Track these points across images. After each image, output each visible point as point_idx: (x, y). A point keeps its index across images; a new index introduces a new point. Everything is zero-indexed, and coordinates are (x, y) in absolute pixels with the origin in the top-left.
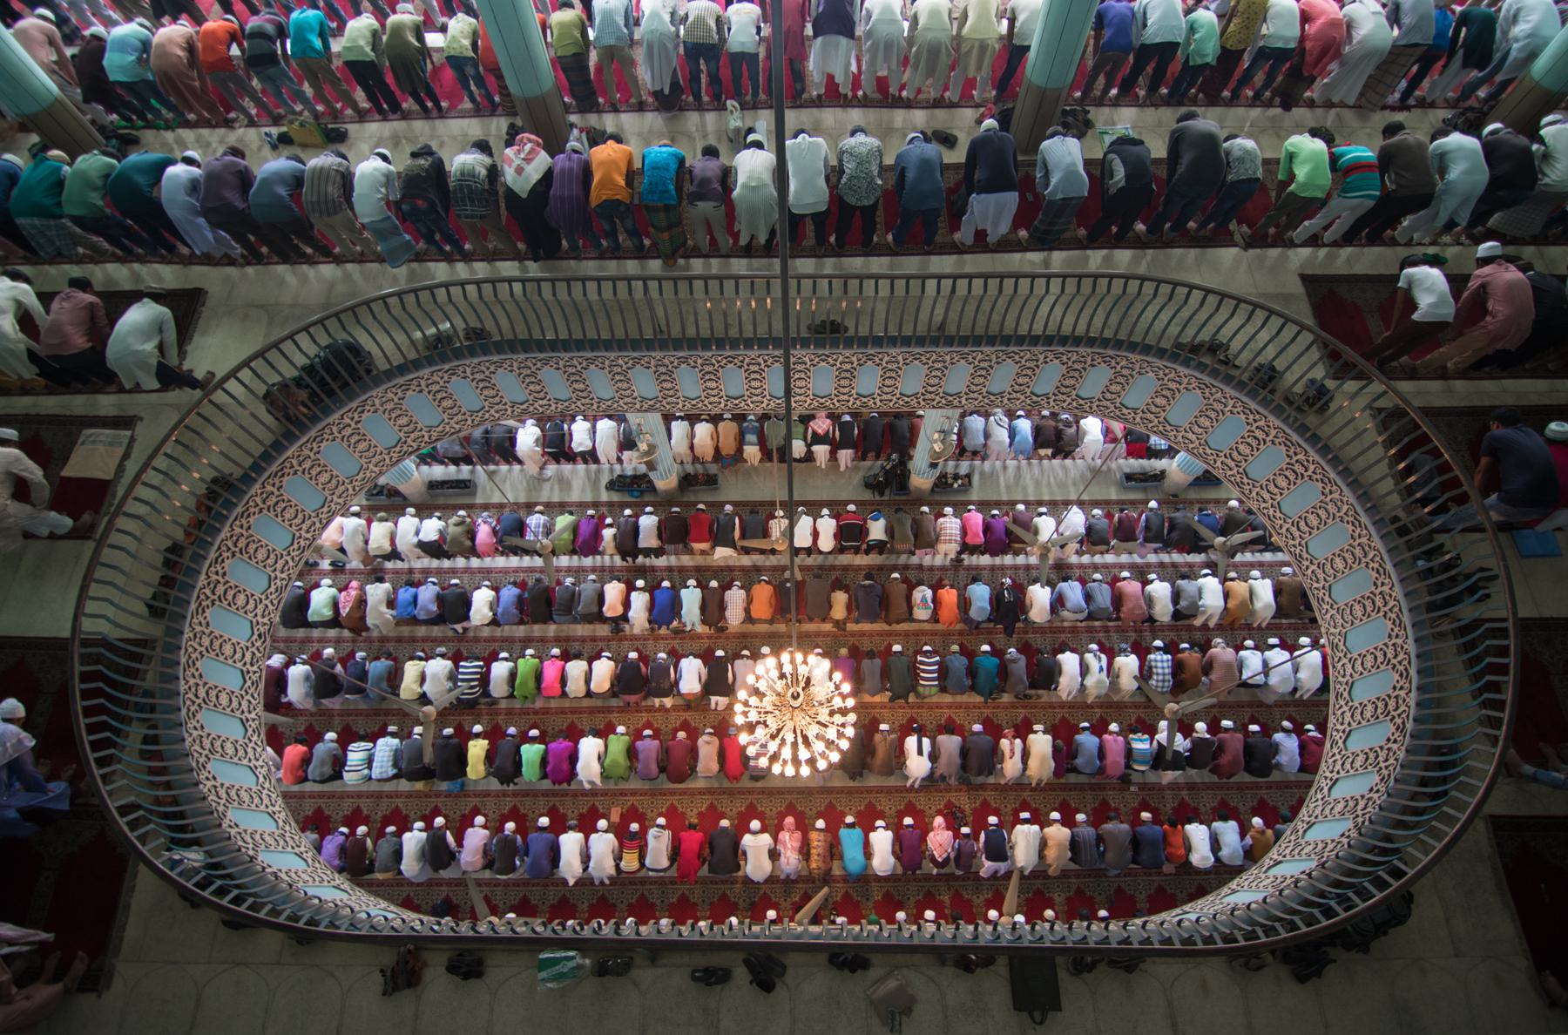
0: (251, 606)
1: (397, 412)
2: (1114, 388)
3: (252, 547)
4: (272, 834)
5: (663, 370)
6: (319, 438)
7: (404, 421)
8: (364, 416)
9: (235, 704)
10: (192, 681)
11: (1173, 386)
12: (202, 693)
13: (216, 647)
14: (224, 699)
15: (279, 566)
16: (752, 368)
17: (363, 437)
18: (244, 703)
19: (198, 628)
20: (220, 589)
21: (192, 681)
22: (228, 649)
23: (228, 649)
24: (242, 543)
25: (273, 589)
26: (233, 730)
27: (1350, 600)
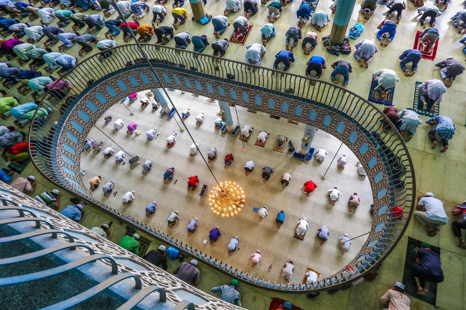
0: (91, 114)
1: (138, 77)
2: (333, 124)
3: (95, 100)
4: (71, 166)
5: (202, 83)
6: (117, 78)
7: (140, 80)
8: (129, 76)
9: (78, 134)
10: (68, 125)
11: (349, 128)
12: (70, 128)
13: (78, 120)
14: (75, 132)
15: (102, 107)
16: (226, 88)
17: (129, 82)
18: (81, 136)
19: (74, 114)
20: (83, 107)
21: (68, 125)
22: (81, 122)
23: (81, 122)
24: (92, 98)
25: (98, 112)
26: (76, 141)
27: (382, 214)
